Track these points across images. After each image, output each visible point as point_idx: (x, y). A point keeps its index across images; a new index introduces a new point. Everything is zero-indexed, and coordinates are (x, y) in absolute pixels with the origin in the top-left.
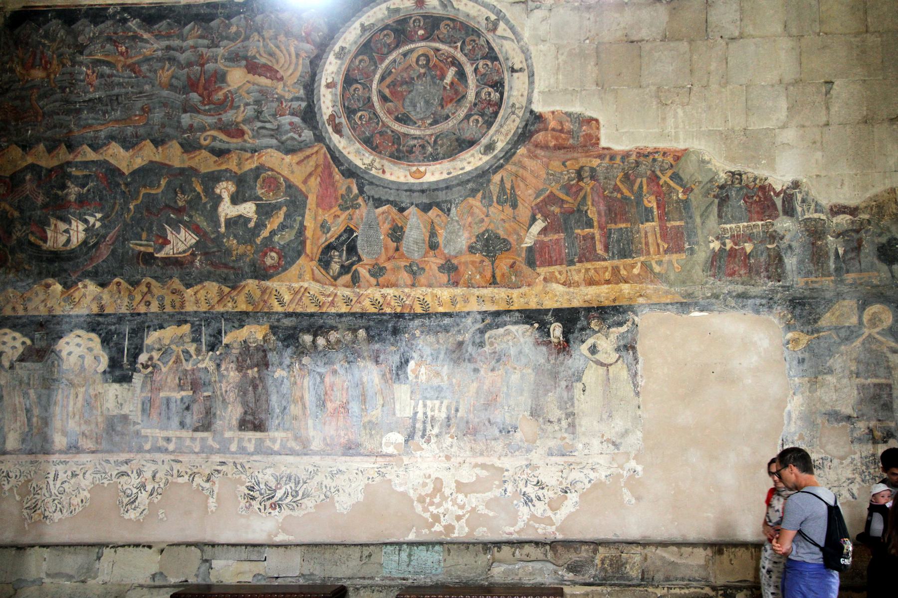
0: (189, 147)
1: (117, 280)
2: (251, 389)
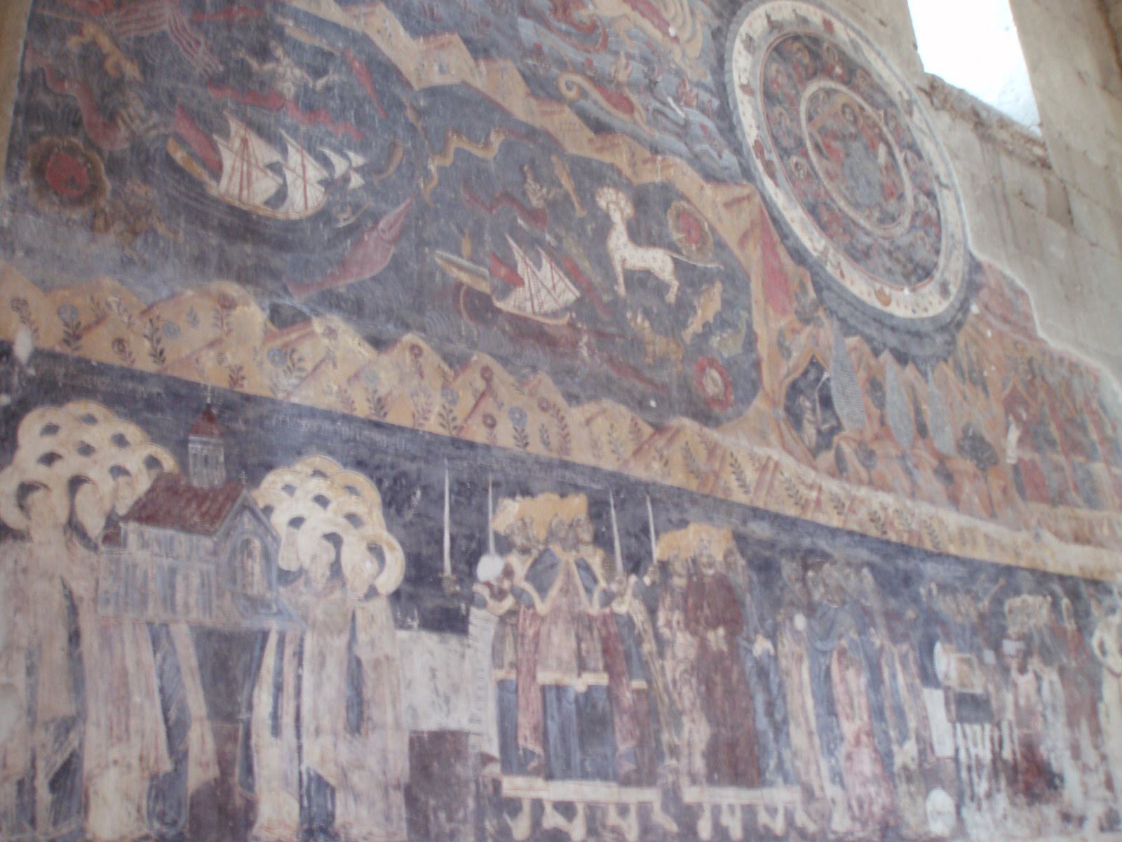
0: (541, 87)
1: (409, 338)
2: (718, 678)
